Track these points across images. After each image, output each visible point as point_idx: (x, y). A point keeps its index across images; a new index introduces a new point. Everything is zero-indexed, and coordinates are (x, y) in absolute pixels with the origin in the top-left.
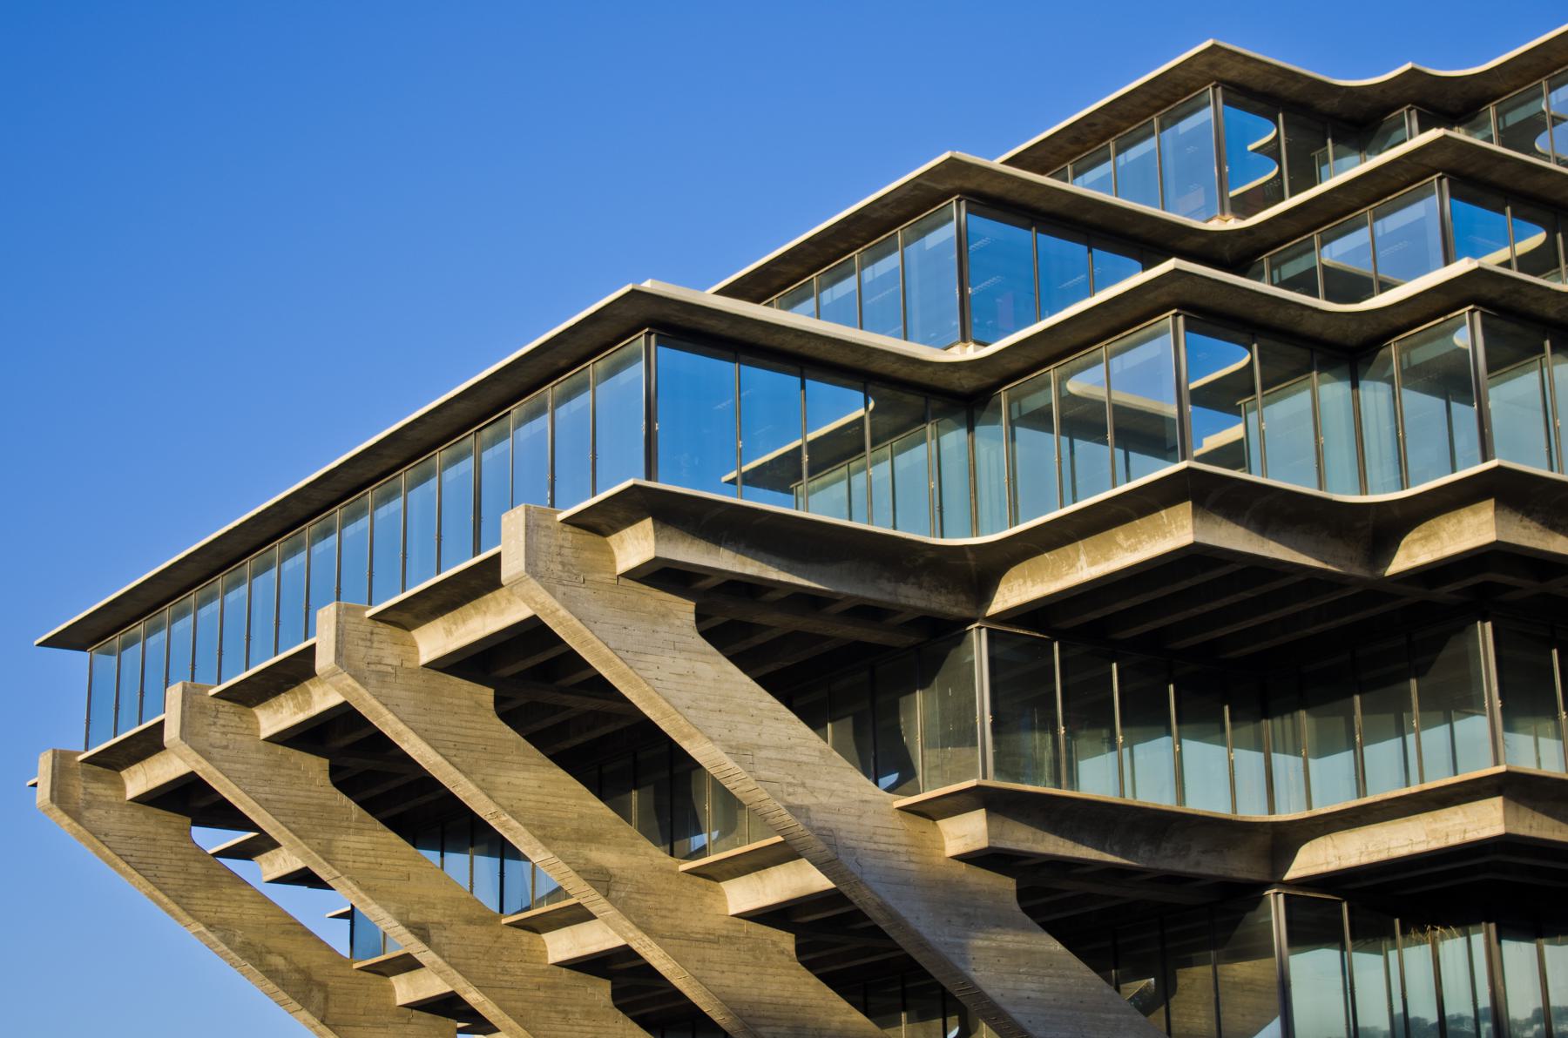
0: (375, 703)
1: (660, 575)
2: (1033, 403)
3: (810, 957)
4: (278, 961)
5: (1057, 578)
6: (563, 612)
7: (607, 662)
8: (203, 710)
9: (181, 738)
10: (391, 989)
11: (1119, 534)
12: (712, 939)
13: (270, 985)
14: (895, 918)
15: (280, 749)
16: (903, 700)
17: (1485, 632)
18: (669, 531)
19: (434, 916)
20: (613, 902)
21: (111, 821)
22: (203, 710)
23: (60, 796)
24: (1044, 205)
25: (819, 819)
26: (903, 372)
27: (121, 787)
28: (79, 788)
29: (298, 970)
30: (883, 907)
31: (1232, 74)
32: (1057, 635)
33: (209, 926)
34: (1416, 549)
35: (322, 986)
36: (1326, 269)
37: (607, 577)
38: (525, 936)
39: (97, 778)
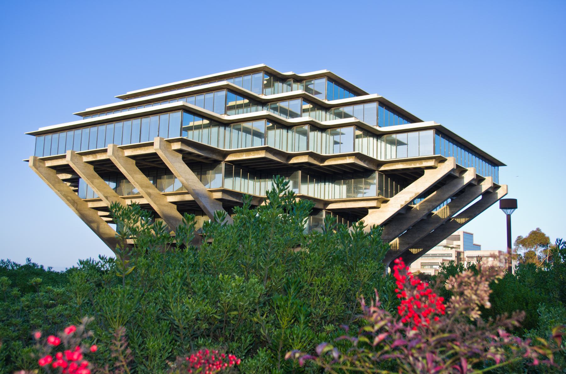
0: (118, 162)
1: (179, 151)
2: (239, 127)
3: (179, 210)
4: (69, 198)
5: (239, 157)
6: (164, 155)
7: (169, 164)
8: (74, 155)
9: (71, 160)
10: (88, 204)
11: (252, 153)
12: (165, 206)
13: (68, 202)
14: (205, 208)
15: (86, 164)
16: (207, 172)
17: (300, 172)
18: (183, 144)
19: (109, 195)
20: (151, 198)
21: (43, 170)
22: (74, 155)
23: (34, 165)
24: (238, 92)
25: (197, 191)
26: (217, 119)
27: (45, 164)
28: (38, 164)
29: (73, 200)
30: (204, 206)
31: (266, 70)
32: (234, 164)
33: (58, 191)
34: (294, 160)
35: (77, 203)
36: (280, 107)
37: (170, 150)
38: (123, 199)
39: (41, 162)
